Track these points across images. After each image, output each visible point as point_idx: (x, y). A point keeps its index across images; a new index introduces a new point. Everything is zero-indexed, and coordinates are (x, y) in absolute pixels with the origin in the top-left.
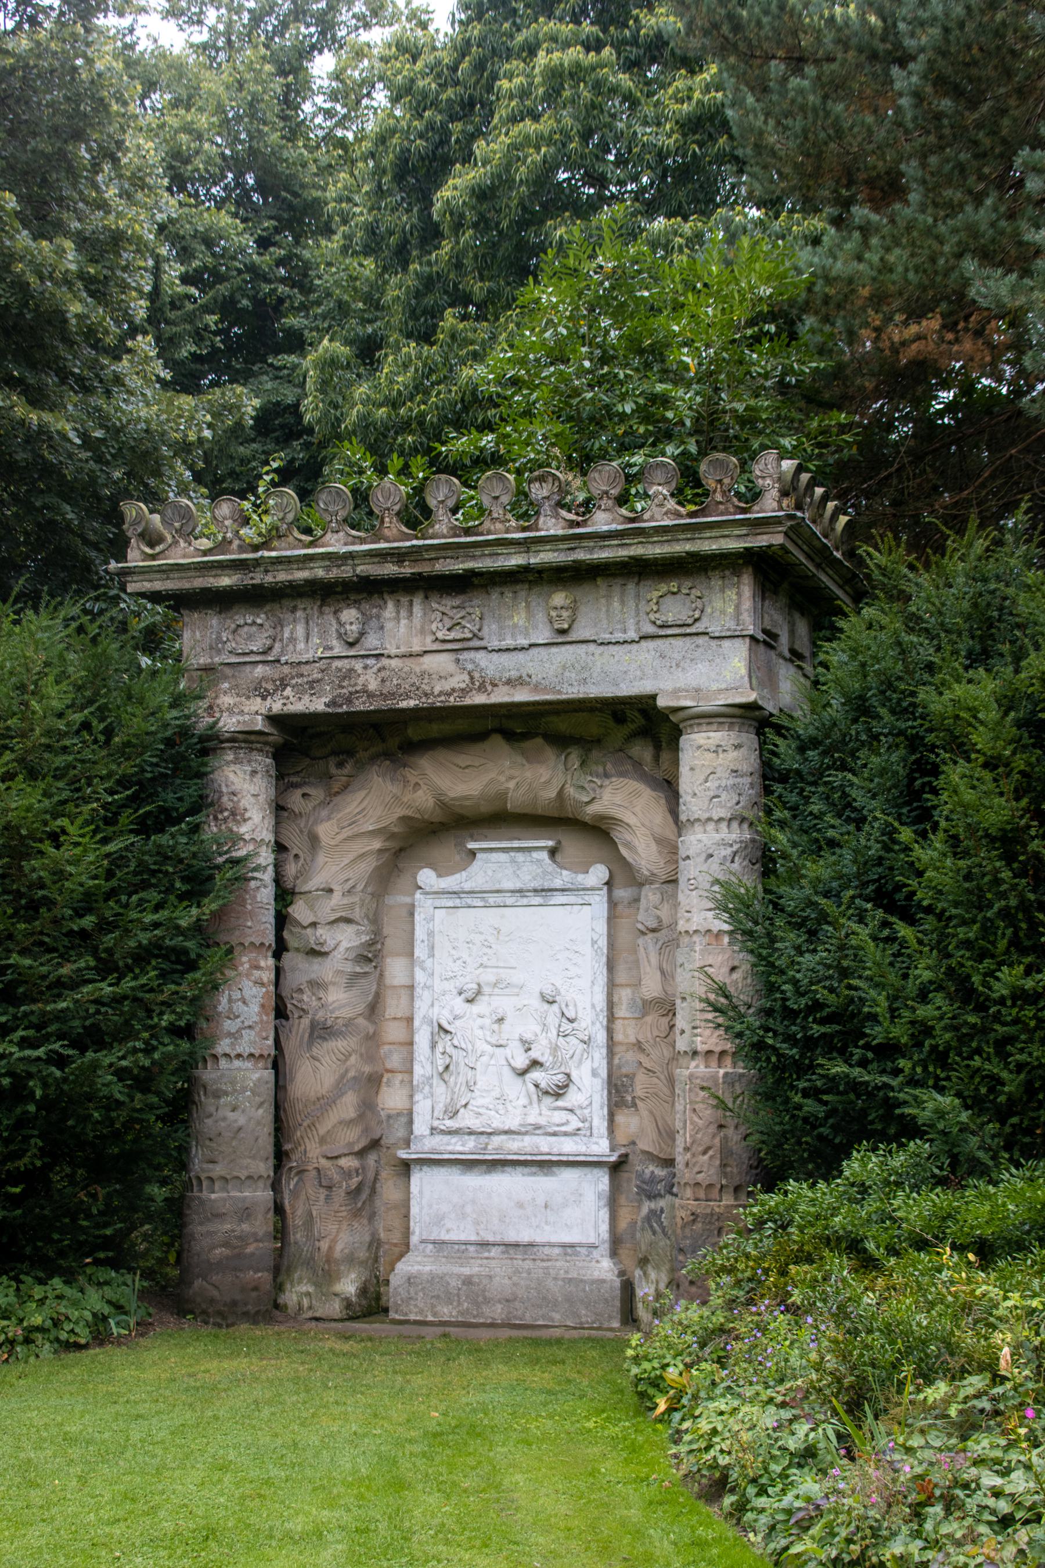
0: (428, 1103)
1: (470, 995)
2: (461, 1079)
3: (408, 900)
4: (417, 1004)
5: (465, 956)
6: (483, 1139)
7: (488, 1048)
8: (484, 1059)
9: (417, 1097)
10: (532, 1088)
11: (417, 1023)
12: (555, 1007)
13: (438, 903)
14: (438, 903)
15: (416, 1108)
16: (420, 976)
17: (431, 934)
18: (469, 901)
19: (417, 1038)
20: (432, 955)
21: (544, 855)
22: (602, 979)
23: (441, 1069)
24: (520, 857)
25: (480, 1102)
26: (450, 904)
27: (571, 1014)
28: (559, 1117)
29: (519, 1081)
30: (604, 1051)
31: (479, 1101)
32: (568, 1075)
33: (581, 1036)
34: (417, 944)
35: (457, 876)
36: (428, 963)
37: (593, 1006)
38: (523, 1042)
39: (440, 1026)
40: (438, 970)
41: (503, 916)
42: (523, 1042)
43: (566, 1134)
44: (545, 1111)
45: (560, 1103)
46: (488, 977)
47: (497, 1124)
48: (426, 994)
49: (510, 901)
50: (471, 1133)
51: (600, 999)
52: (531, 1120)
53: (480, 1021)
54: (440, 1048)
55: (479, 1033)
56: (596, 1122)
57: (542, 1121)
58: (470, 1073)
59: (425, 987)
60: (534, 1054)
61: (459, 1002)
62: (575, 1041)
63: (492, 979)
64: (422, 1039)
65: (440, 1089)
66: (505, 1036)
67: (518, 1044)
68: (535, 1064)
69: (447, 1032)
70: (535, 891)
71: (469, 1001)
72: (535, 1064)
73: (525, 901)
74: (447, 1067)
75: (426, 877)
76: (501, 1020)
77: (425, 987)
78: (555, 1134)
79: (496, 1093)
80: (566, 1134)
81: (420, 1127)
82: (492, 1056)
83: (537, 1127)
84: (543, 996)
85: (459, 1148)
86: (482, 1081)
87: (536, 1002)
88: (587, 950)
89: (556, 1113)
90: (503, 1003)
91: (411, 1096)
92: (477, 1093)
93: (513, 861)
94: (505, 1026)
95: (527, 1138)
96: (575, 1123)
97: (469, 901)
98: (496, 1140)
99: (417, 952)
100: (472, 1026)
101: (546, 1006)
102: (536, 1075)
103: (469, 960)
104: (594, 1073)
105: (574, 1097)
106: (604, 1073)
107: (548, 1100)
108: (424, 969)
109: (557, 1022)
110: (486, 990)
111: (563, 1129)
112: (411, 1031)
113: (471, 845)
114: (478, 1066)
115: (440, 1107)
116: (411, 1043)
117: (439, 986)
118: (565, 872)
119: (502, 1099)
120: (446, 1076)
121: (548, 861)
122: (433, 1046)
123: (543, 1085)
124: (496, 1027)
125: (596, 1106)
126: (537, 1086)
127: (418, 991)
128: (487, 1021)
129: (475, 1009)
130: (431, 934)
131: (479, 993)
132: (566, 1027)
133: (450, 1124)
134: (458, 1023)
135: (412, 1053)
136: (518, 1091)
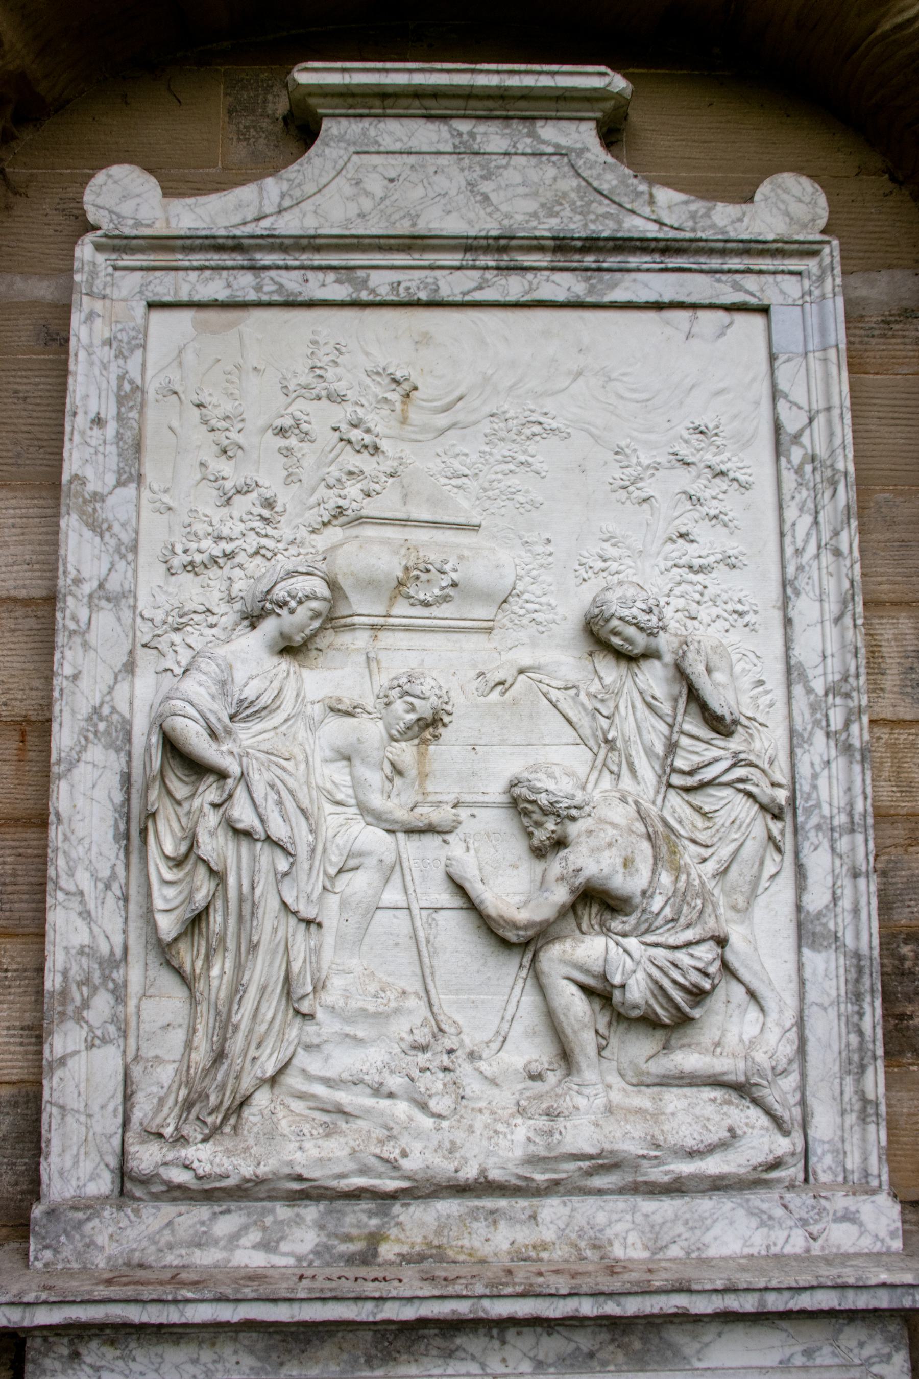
0: (109, 1061)
1: (296, 620)
2: (263, 970)
3: (42, 290)
4: (68, 659)
5: (271, 482)
6: (358, 1218)
7: (374, 839)
8: (359, 883)
9: (63, 1041)
10: (575, 1006)
11: (63, 738)
12: (653, 678)
13: (165, 286)
14: (165, 286)
15: (60, 1088)
16: (82, 553)
17: (130, 396)
18: (292, 282)
19: (63, 798)
20: (131, 475)
21: (583, 135)
22: (828, 582)
23: (167, 925)
24: (493, 137)
25: (344, 1061)
26: (214, 288)
27: (719, 699)
28: (690, 1116)
29: (507, 972)
30: (860, 848)
31: (341, 1059)
32: (722, 942)
33: (764, 791)
34: (77, 426)
35: (247, 193)
36: (118, 507)
37: (792, 672)
38: (522, 806)
39: (174, 750)
40: (155, 533)
41: (424, 340)
42: (522, 806)
43: (718, 1185)
44: (622, 1095)
45: (688, 1060)
46: (373, 555)
47: (421, 1158)
48: (105, 622)
49: (453, 285)
50: (305, 1192)
51: (824, 641)
52: (581, 1135)
53: (337, 730)
54: (167, 839)
55: (338, 774)
56: (825, 1124)
57: (628, 1139)
58: (301, 942)
59: (103, 595)
60: (592, 858)
61: (250, 656)
62: (744, 809)
63: (390, 565)
64: (85, 802)
65: (162, 1007)
66: (444, 788)
67: (497, 821)
68: (596, 902)
69: (197, 768)
70: (561, 245)
71: (290, 649)
72: (596, 902)
73: (514, 287)
74: (197, 921)
75: (122, 194)
76: (429, 725)
77: (103, 595)
78: (676, 1188)
79: (411, 1022)
80: (718, 1185)
81: (73, 1167)
82: (392, 869)
83: (605, 1163)
84: (601, 638)
85: (249, 1258)
86: (351, 971)
87: (566, 661)
88: (757, 463)
89: (675, 1100)
90: (440, 663)
91: (36, 1034)
92: (327, 1025)
93: (466, 151)
94: (447, 751)
95: (552, 1210)
96: (760, 1142)
97: (292, 282)
98: (417, 1223)
99: (74, 461)
100: (304, 743)
101: (610, 672)
102: (591, 948)
103: (285, 498)
104: (806, 931)
105: (735, 1034)
106: (866, 936)
107: (639, 1049)
108: (98, 527)
109: (656, 733)
110: (362, 606)
111: (713, 1166)
112: (40, 771)
113: (310, 75)
114: (331, 916)
115: (160, 1079)
116: (40, 820)
117: (155, 591)
118: (665, 196)
119: (434, 1043)
120: (188, 956)
121: (597, 151)
122: (134, 831)
123: (637, 992)
124: (405, 752)
125: (824, 1059)
126: (600, 992)
127: (73, 610)
128: (371, 731)
129: (316, 681)
130: (130, 396)
131: (331, 620)
132: (699, 750)
133: (206, 1157)
134: (248, 735)
135: (41, 858)
136: (491, 1008)
